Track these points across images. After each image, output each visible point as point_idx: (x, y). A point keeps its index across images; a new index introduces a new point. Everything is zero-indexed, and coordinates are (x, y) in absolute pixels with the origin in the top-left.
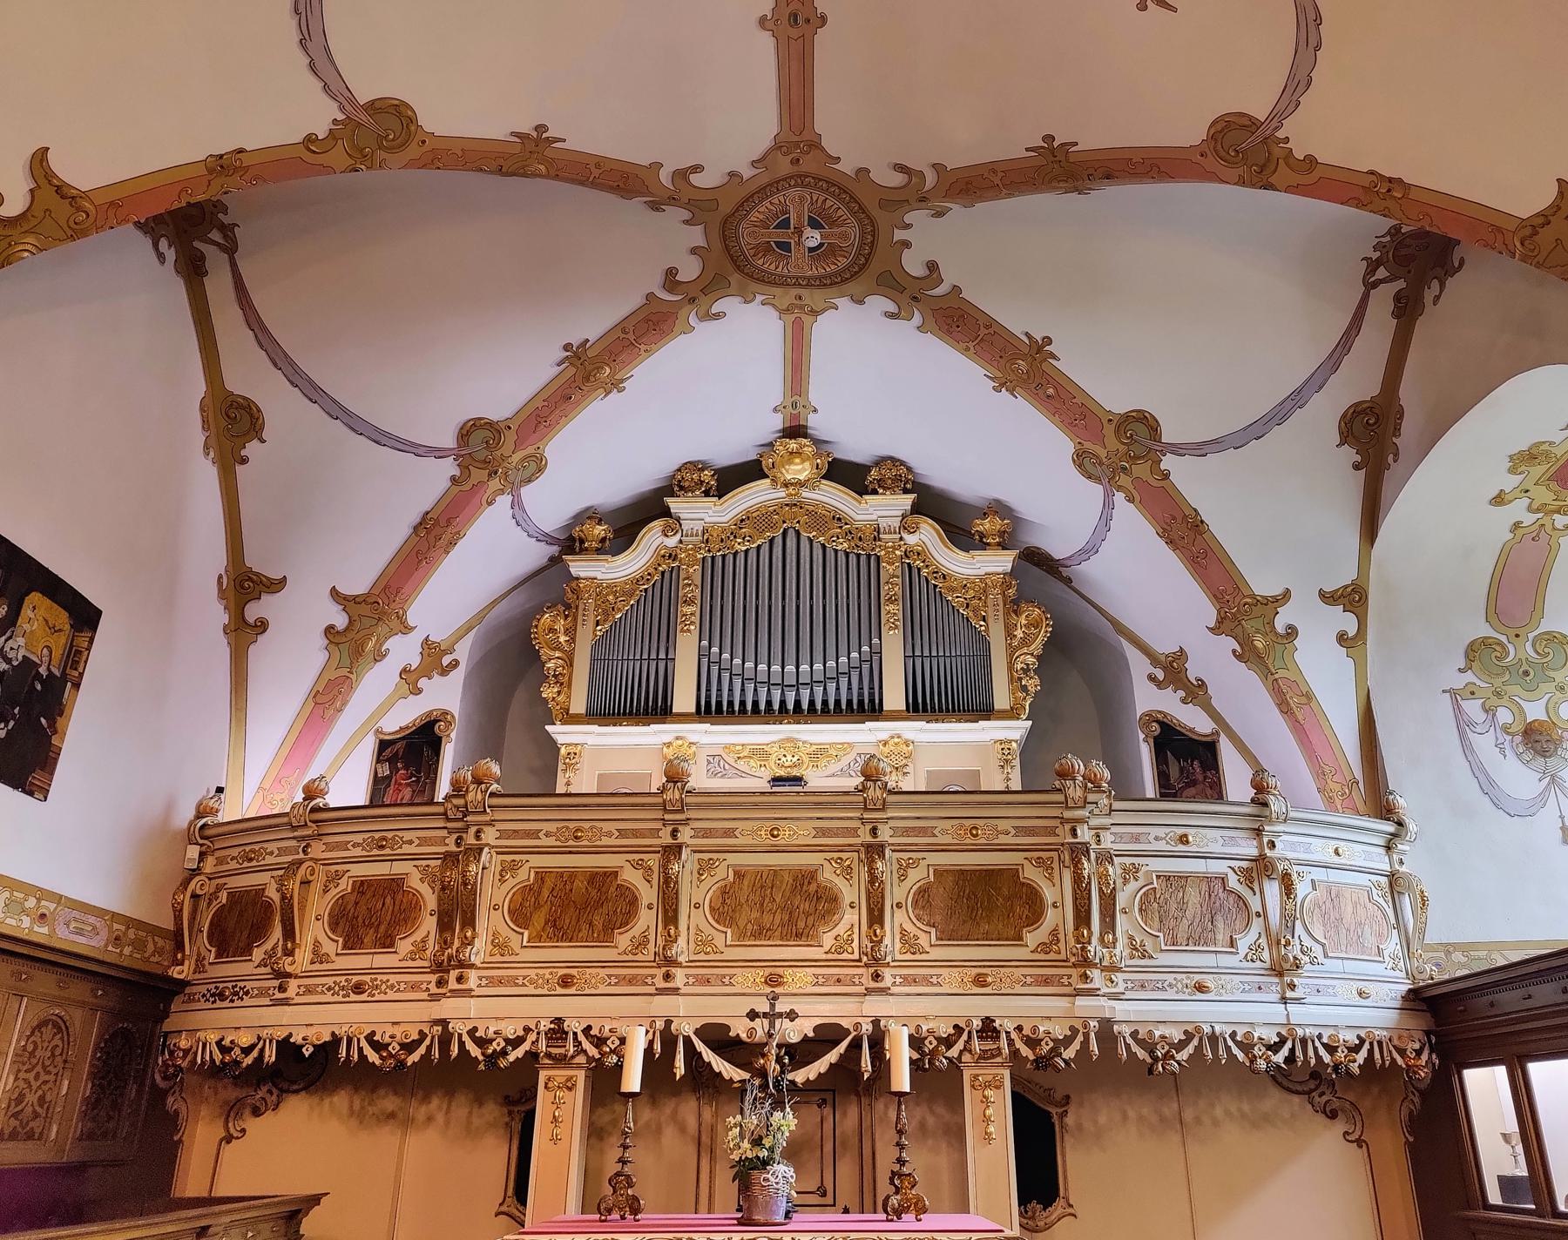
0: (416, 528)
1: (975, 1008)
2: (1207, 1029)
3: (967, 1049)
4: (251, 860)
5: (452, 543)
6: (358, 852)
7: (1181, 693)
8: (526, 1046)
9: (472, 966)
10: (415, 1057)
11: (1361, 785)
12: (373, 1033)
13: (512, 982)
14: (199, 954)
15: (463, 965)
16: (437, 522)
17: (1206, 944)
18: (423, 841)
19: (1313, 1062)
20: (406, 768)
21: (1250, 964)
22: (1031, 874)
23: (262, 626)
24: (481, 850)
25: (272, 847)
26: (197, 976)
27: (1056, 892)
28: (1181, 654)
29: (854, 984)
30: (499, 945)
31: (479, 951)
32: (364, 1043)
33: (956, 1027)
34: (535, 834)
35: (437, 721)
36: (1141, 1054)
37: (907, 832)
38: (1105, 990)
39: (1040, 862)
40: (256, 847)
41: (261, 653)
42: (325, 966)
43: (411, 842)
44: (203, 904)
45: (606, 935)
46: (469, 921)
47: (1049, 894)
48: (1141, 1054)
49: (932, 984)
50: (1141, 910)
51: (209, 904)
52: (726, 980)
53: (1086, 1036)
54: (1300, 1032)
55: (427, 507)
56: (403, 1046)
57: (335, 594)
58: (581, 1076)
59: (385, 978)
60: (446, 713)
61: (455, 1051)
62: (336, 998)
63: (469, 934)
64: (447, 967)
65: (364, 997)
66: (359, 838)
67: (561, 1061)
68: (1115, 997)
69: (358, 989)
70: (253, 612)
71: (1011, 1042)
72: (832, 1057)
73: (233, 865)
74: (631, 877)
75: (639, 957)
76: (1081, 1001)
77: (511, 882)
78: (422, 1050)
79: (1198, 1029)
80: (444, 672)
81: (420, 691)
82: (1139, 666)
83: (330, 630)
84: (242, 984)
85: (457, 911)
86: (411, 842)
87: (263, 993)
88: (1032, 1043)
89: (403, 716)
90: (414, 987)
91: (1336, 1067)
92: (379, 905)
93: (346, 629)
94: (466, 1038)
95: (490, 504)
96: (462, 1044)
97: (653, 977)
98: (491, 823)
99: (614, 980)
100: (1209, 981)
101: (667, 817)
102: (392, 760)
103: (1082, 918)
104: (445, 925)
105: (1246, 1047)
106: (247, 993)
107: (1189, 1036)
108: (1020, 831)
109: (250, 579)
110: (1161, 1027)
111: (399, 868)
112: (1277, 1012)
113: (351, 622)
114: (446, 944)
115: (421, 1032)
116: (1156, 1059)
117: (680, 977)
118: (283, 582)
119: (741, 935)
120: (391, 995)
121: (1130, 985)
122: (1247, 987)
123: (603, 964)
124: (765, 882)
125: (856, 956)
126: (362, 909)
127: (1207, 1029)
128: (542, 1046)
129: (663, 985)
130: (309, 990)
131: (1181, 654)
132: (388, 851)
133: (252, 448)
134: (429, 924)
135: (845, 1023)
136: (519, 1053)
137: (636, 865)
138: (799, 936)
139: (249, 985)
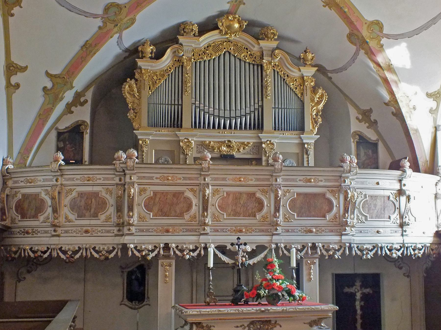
0: (82, 47)
1: (309, 239)
2: (380, 245)
3: (307, 253)
4: (31, 183)
5: (95, 54)
6: (78, 182)
7: (367, 124)
8: (156, 252)
9: (133, 225)
10: (112, 255)
11: (428, 163)
12: (95, 247)
13: (148, 231)
14: (12, 218)
15: (130, 224)
16: (91, 45)
17: (381, 218)
18: (105, 179)
19: (409, 254)
20: (70, 144)
21: (394, 224)
22: (329, 196)
23: (17, 86)
24: (134, 184)
25: (39, 178)
26: (13, 225)
27: (338, 203)
28: (371, 111)
29: (268, 232)
30: (141, 218)
31: (135, 220)
32: (92, 251)
33: (303, 246)
34: (151, 178)
35: (80, 125)
36: (359, 253)
37: (287, 180)
38: (351, 234)
39: (332, 192)
40: (33, 178)
41: (16, 96)
42: (71, 223)
43: (100, 179)
44: (10, 199)
45: (181, 215)
46: (131, 209)
47: (335, 202)
48: (359, 253)
49: (295, 232)
50: (362, 207)
51: (13, 198)
52: (225, 230)
53: (345, 248)
54: (406, 245)
55: (87, 39)
56: (107, 252)
57: (47, 73)
58: (173, 262)
59: (96, 228)
60: (84, 122)
61: (130, 253)
62: (77, 235)
63: (131, 214)
64: (121, 226)
65: (89, 235)
66: (78, 177)
67: (167, 257)
68: (353, 235)
69: (87, 232)
70: (14, 80)
71: (321, 250)
72: (262, 255)
73: (22, 184)
74: (189, 194)
75: (193, 222)
76: (343, 237)
77: (144, 196)
78: (114, 253)
79: (377, 245)
80: (82, 104)
81: (72, 112)
82: (353, 113)
83: (45, 89)
84: (36, 229)
85: (123, 205)
86: (100, 179)
87: (46, 232)
88: (327, 250)
89: (66, 123)
90: (108, 232)
91: (415, 254)
92: (90, 202)
93: (52, 88)
94: (133, 250)
95: (111, 37)
96: (132, 252)
97: (199, 229)
98: (134, 174)
99: (185, 230)
100: (381, 230)
101: (202, 173)
102: (64, 141)
103: (346, 210)
104: (119, 209)
105: (390, 250)
106: (39, 232)
107: (374, 247)
108: (326, 180)
109: (13, 66)
110: (366, 245)
111: (96, 189)
112: (400, 239)
113: (53, 86)
114: (119, 217)
115: (113, 247)
116: (363, 255)
117: (208, 229)
118: (26, 68)
119: (229, 215)
120: (99, 234)
121: (357, 232)
122: (392, 232)
123: (181, 225)
124: (237, 196)
125: (269, 223)
126: (83, 203)
127: (380, 245)
128: (162, 252)
129: (202, 232)
130: (66, 232)
131: (371, 111)
132: (91, 182)
133: (16, 10)
134: (111, 210)
135: (266, 245)
136: (154, 254)
137: (192, 190)
138: (249, 216)
139: (39, 229)
